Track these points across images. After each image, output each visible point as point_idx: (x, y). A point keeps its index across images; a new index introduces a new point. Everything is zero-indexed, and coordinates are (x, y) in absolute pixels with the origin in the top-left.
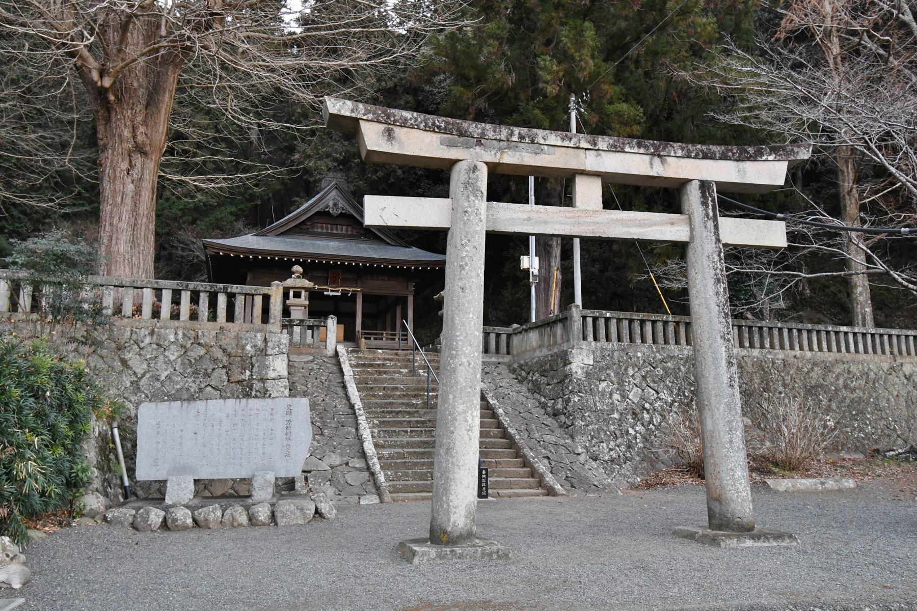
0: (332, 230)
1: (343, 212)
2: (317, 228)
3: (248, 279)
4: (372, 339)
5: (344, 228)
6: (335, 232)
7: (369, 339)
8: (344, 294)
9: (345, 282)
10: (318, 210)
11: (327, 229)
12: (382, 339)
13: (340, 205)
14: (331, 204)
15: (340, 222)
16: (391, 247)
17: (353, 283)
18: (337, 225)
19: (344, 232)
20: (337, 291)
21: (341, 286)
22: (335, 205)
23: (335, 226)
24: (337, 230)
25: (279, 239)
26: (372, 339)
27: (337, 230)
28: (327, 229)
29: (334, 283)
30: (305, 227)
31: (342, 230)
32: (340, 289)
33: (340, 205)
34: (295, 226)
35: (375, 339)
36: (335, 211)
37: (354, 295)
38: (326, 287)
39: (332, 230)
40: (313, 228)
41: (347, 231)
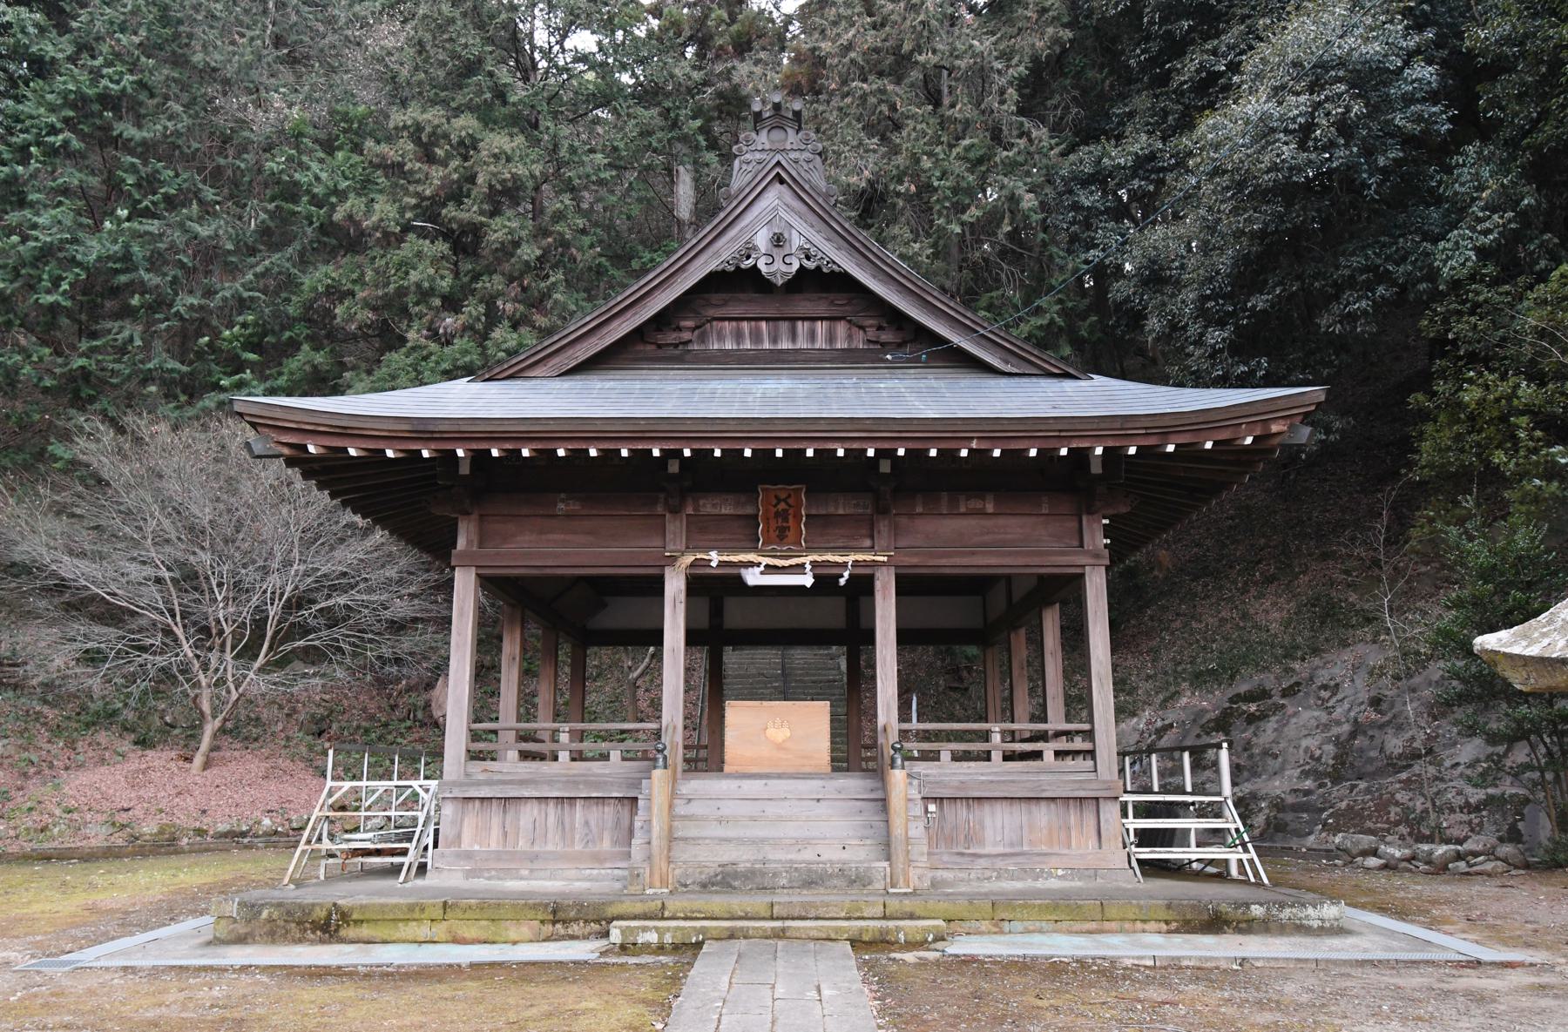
0: (774, 340)
1: (810, 265)
2: (721, 338)
3: (461, 543)
4: (945, 756)
5: (821, 328)
6: (785, 345)
7: (934, 756)
8: (825, 582)
9: (824, 529)
10: (713, 265)
11: (756, 337)
12: (987, 757)
13: (796, 241)
14: (762, 240)
15: (804, 306)
16: (1003, 382)
17: (863, 529)
18: (793, 320)
19: (820, 343)
20: (799, 569)
21: (810, 549)
22: (778, 241)
23: (784, 326)
24: (793, 336)
25: (559, 384)
26: (945, 756)
27: (793, 336)
28: (756, 337)
29: (781, 536)
30: (672, 337)
31: (812, 336)
32: (807, 560)
33: (796, 241)
34: (638, 334)
35: (957, 757)
36: (779, 266)
37: (863, 586)
38: (752, 557)
39: (774, 340)
40: (703, 339)
41: (831, 338)
